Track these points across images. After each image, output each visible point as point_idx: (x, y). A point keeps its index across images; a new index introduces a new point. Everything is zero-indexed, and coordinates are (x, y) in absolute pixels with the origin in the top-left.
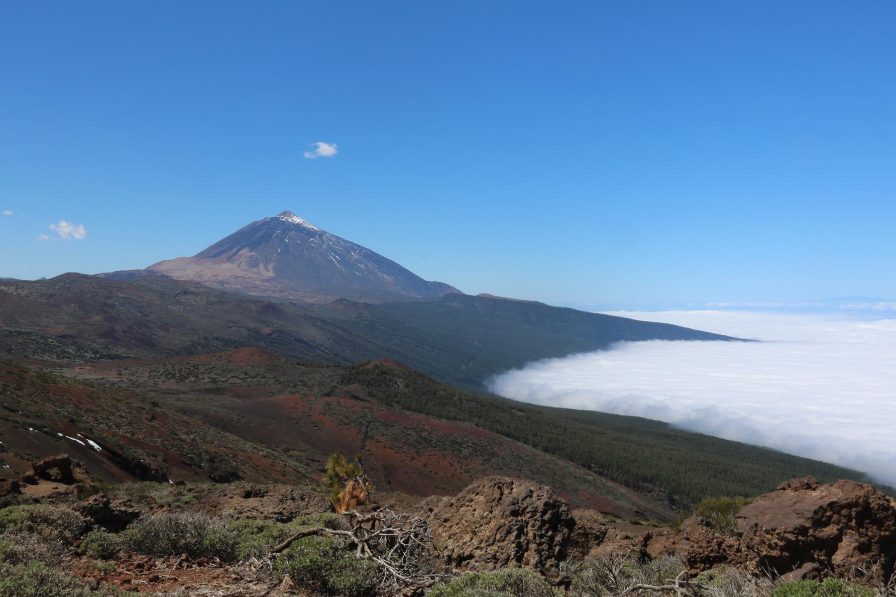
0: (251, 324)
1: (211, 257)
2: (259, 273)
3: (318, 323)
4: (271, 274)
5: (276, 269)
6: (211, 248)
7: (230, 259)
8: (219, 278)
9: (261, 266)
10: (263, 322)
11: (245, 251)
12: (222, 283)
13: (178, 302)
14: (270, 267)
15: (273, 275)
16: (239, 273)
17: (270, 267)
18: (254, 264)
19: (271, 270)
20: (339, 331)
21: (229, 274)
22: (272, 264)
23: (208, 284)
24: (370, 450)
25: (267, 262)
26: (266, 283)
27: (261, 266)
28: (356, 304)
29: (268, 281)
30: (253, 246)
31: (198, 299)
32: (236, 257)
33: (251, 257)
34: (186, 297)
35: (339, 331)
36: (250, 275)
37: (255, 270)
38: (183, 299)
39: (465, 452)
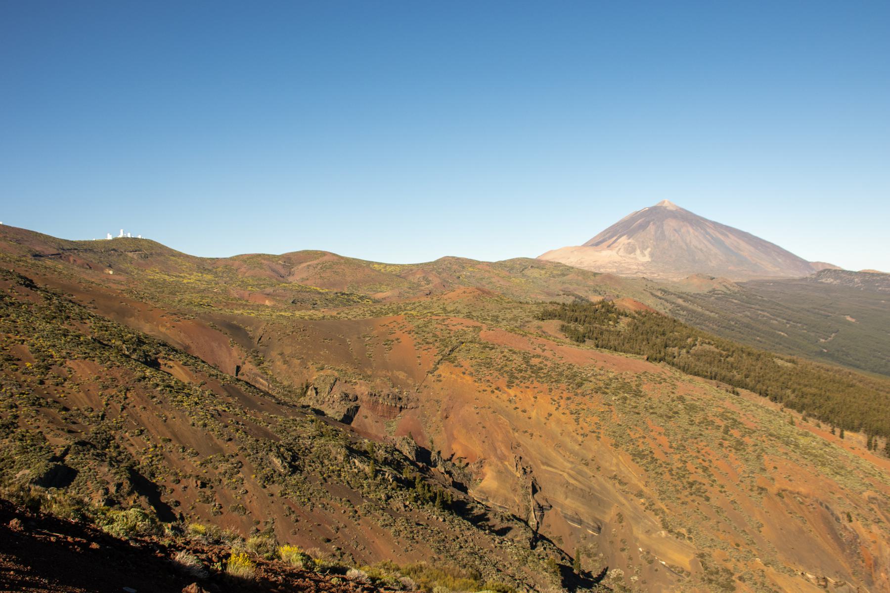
0: (582, 294)
1: (592, 245)
2: (636, 259)
3: (659, 294)
4: (647, 259)
5: (652, 255)
7: (609, 246)
8: (598, 264)
9: (638, 252)
10: (595, 291)
11: (624, 240)
12: (599, 267)
13: (524, 276)
14: (647, 252)
15: (650, 260)
16: (617, 258)
18: (631, 250)
19: (648, 256)
20: (680, 301)
21: (607, 260)
22: (649, 249)
23: (586, 269)
24: (440, 376)
25: (643, 249)
26: (641, 268)
27: (638, 252)
28: (712, 279)
29: (643, 265)
30: (631, 233)
31: (543, 272)
32: (615, 245)
33: (629, 244)
34: (532, 270)
35: (680, 301)
36: (627, 260)
37: (632, 255)
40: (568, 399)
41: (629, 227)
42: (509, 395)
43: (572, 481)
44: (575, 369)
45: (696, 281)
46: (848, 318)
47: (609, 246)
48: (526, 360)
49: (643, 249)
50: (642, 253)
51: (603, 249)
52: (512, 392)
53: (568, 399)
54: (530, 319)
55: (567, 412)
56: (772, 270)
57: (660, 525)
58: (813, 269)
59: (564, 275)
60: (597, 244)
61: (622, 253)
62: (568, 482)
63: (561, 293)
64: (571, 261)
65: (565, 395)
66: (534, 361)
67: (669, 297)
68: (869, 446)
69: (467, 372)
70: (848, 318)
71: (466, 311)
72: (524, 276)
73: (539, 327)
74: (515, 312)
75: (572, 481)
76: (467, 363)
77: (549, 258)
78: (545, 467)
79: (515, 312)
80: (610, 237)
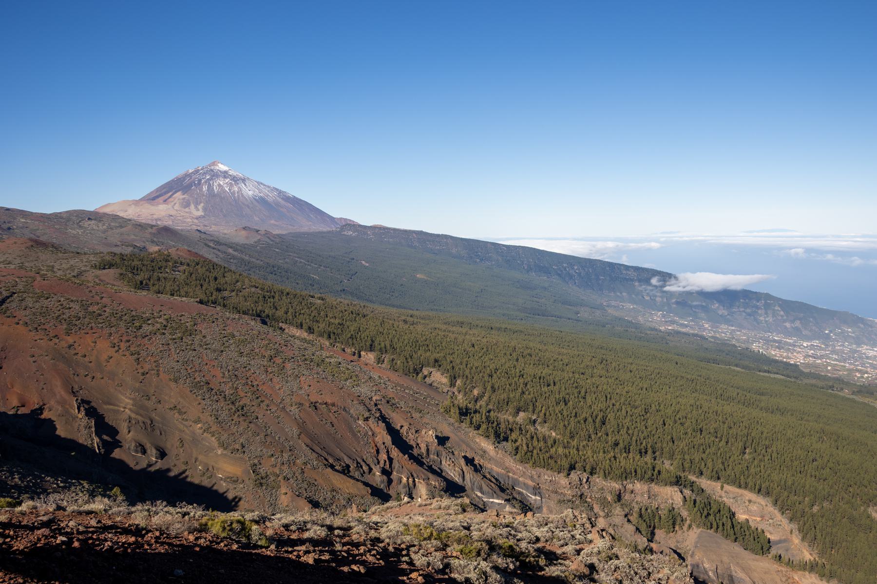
2: (190, 213)
3: (211, 245)
4: (201, 213)
5: (205, 209)
6: (152, 192)
7: (165, 201)
8: (155, 217)
9: (192, 206)
10: (153, 242)
11: (179, 195)
14: (200, 207)
16: (173, 213)
17: (200, 207)
18: (186, 204)
20: (230, 251)
21: (162, 213)
22: (202, 205)
23: (143, 221)
25: (197, 204)
26: (195, 221)
27: (192, 206)
28: (257, 231)
31: (100, 225)
32: (171, 199)
34: (89, 222)
35: (230, 251)
37: (187, 210)
38: (86, 224)
39: (146, 328)
40: (128, 341)
41: (181, 185)
42: (67, 342)
43: (133, 415)
44: (134, 313)
45: (243, 233)
46: (363, 262)
47: (165, 201)
48: (85, 306)
49: (197, 204)
50: (196, 207)
51: (160, 204)
52: (70, 340)
53: (128, 341)
54: (88, 268)
55: (127, 353)
56: (307, 226)
57: (216, 444)
58: (337, 224)
59: (121, 227)
60: (154, 199)
61: (177, 207)
62: (130, 417)
63: (119, 243)
64: (130, 213)
65: (125, 338)
66: (94, 308)
67: (220, 248)
68: (380, 361)
69: (21, 322)
70: (363, 262)
71: (18, 261)
72: (80, 227)
73: (97, 277)
74: (72, 262)
75: (133, 415)
76: (21, 314)
77: (108, 210)
78: (105, 407)
79: (72, 262)
80: (166, 193)
